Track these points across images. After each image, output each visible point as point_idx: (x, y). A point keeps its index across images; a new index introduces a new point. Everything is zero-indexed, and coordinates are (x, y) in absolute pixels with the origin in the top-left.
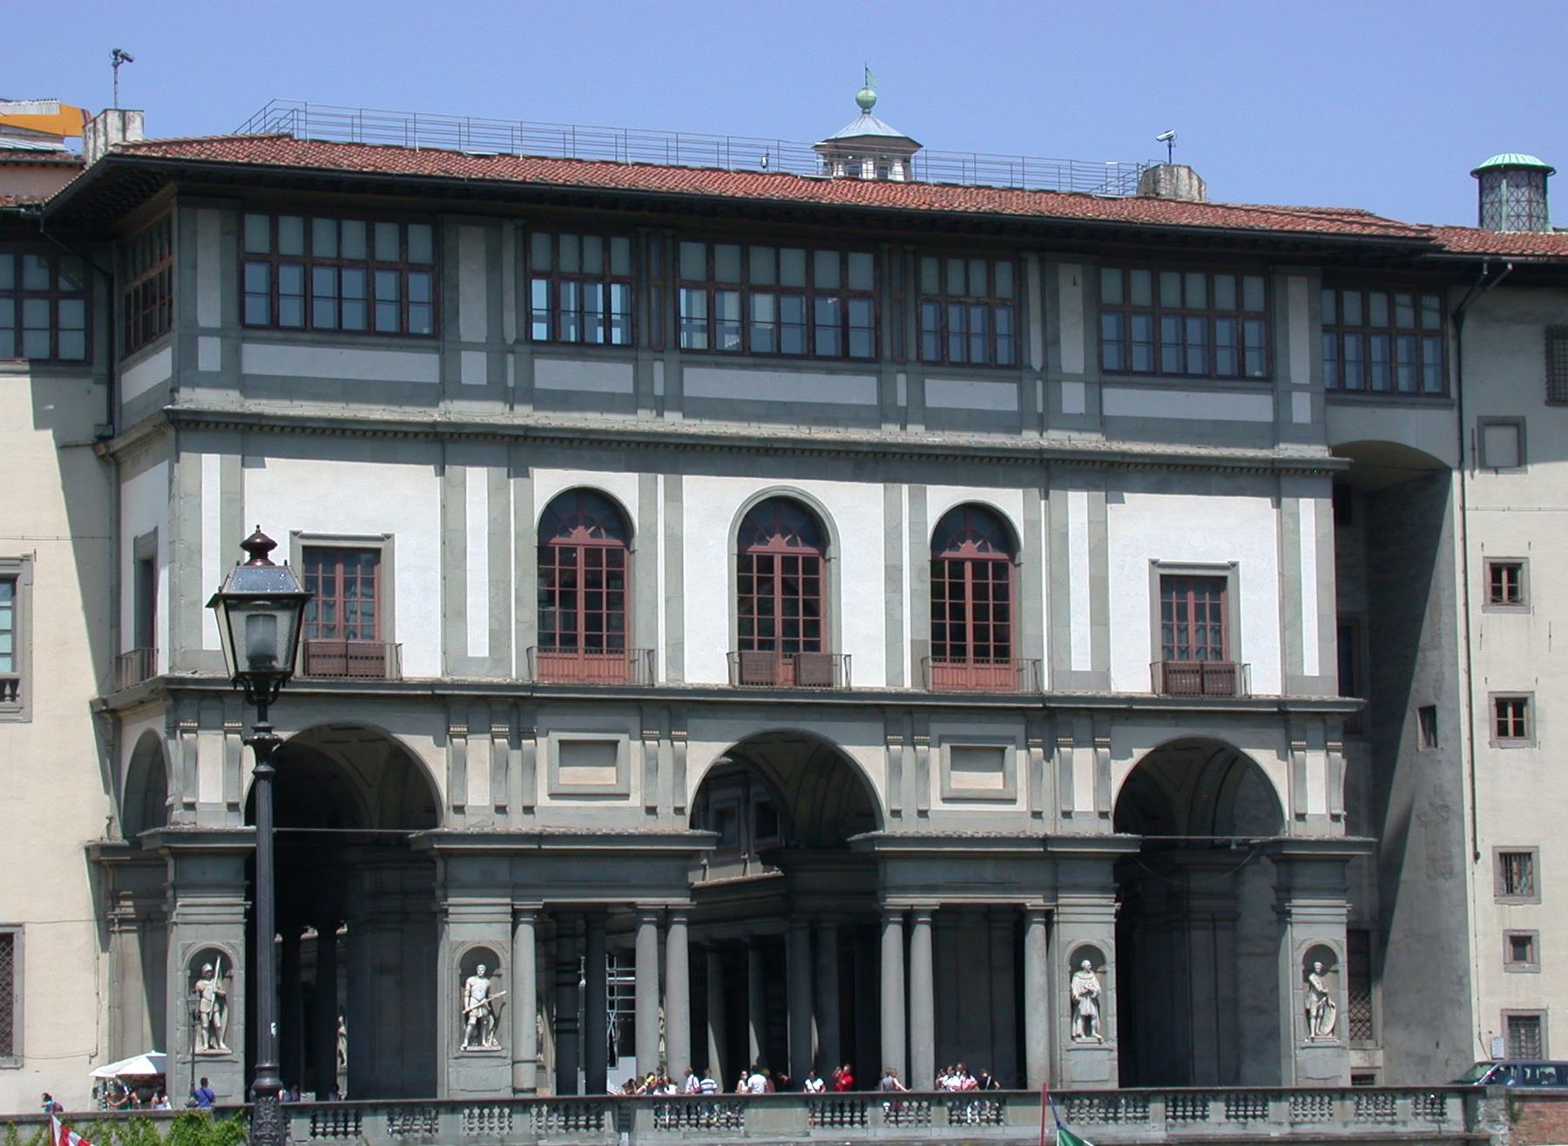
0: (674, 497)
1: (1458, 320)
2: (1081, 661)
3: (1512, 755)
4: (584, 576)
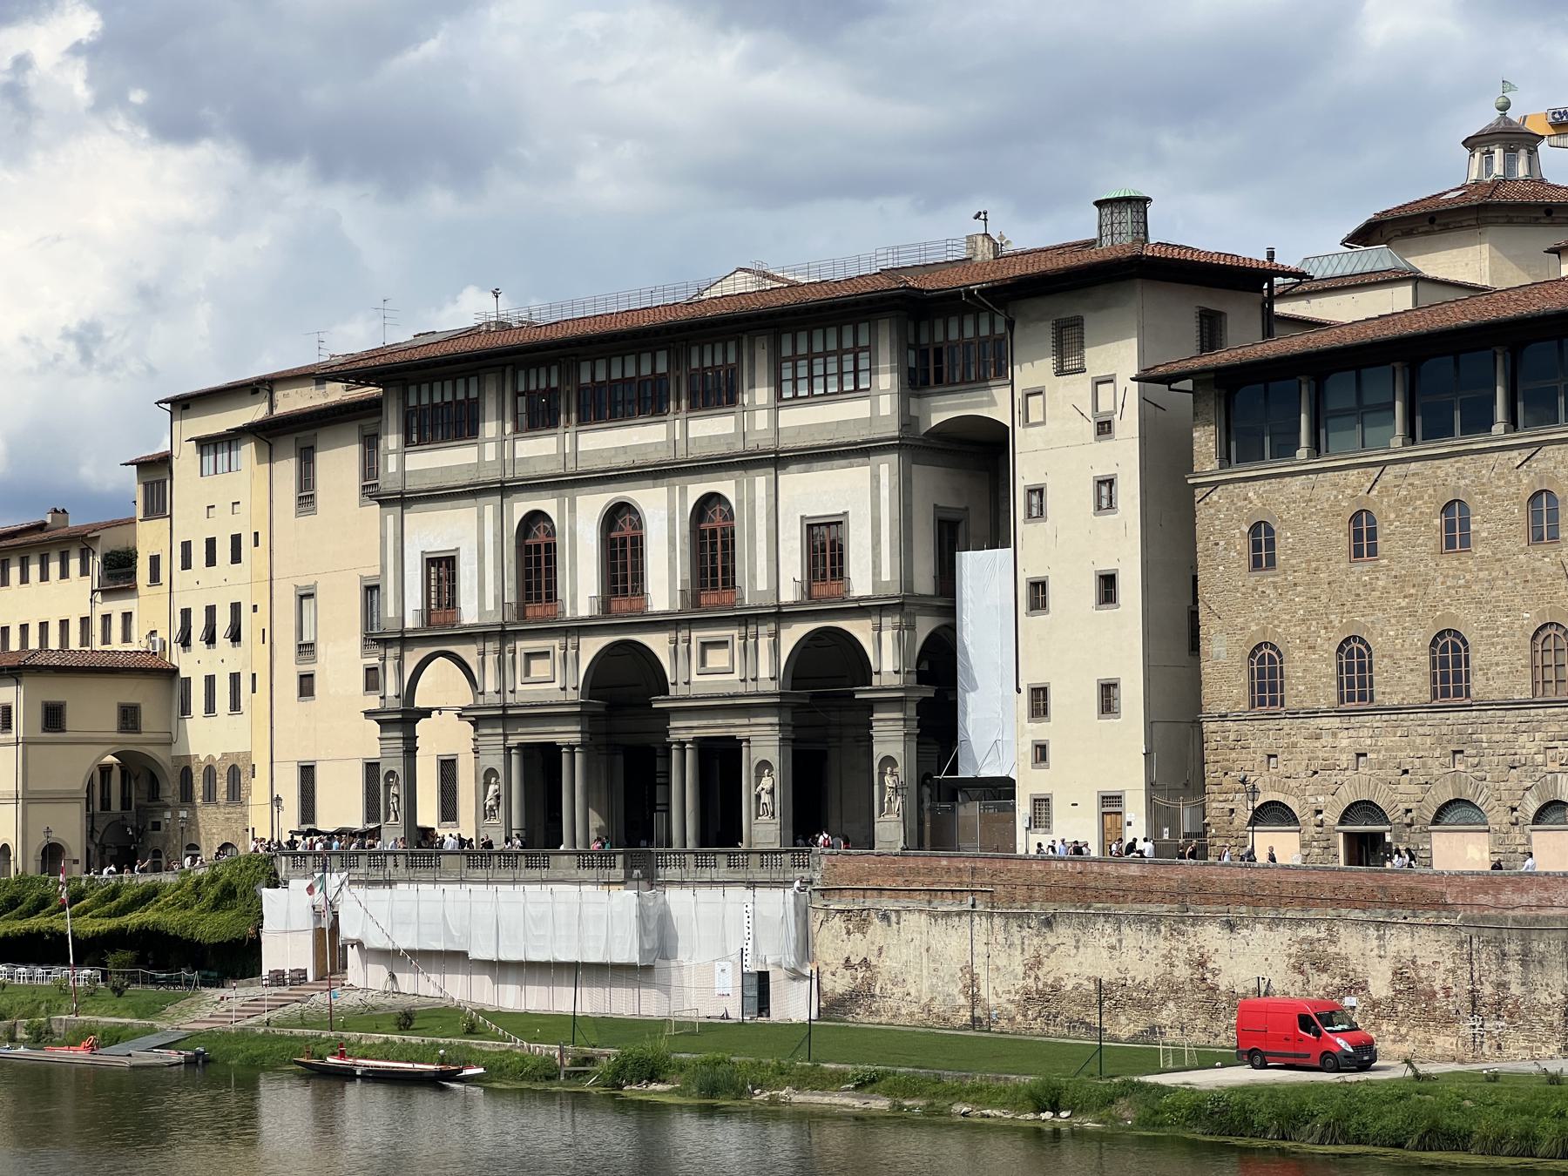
1: (1010, 325)
2: (762, 584)
3: (1040, 619)
4: (536, 557)
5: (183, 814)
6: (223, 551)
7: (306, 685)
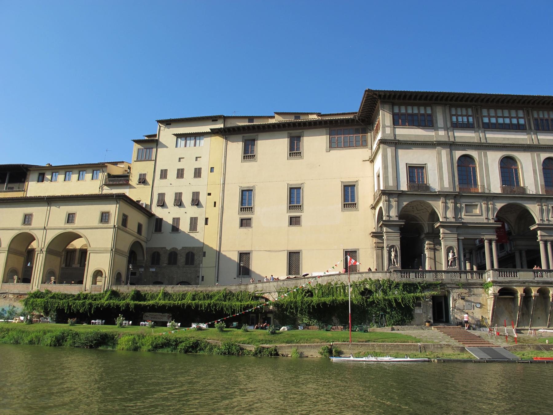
0: (486, 156)
5: (154, 270)
6: (189, 174)
7: (245, 223)
